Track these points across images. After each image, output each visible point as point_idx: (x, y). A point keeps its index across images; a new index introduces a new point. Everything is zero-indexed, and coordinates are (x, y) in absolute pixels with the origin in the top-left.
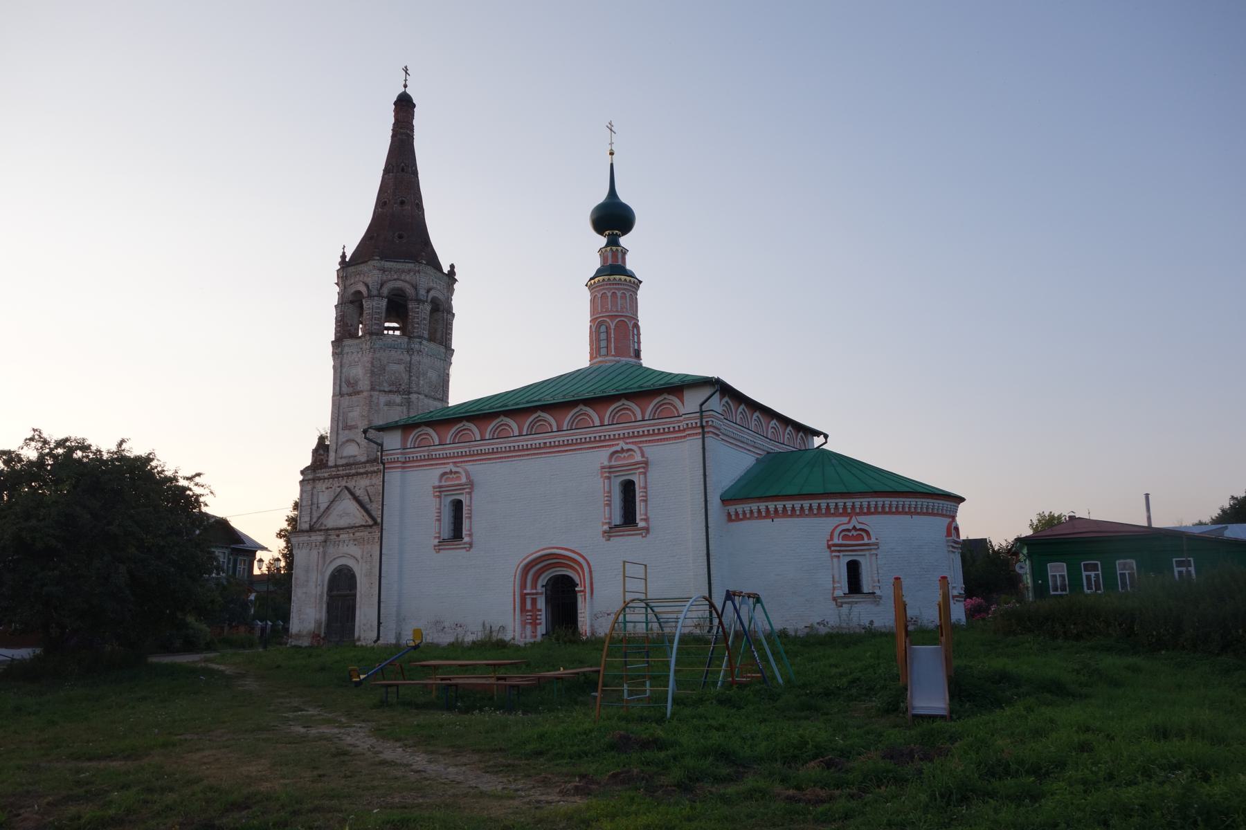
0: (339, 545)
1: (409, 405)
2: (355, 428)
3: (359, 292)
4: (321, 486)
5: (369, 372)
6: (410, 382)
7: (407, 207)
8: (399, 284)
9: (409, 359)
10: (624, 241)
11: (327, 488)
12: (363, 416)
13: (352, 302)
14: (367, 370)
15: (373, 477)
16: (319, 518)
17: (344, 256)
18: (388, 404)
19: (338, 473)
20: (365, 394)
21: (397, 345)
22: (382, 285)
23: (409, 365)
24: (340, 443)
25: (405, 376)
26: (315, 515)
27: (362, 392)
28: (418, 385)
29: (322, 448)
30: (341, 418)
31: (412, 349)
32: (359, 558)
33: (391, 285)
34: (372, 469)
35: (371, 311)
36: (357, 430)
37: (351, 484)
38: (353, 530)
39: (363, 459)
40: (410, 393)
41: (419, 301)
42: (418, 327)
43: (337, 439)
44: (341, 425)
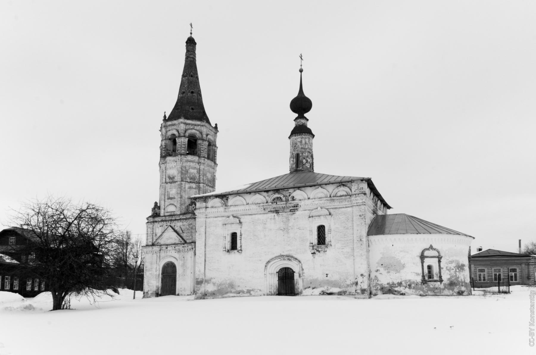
0: (167, 252)
1: (199, 189)
2: (174, 199)
3: (174, 135)
4: (156, 224)
5: (180, 172)
6: (199, 179)
7: (195, 94)
8: (194, 131)
9: (199, 167)
11: (161, 226)
12: (177, 193)
13: (170, 139)
14: (179, 172)
15: (184, 222)
16: (157, 240)
17: (165, 116)
18: (190, 188)
19: (166, 219)
20: (179, 183)
21: (194, 160)
22: (185, 132)
23: (199, 170)
24: (166, 206)
25: (197, 176)
26: (155, 238)
27: (177, 182)
28: (203, 179)
29: (157, 207)
30: (166, 194)
31: (200, 163)
32: (178, 259)
33: (189, 132)
34: (183, 218)
35: (180, 144)
36: (175, 200)
37: (173, 225)
38: (174, 246)
39: (179, 213)
40: (199, 183)
41: (203, 140)
42: (203, 153)
43: (165, 204)
44: (166, 197)
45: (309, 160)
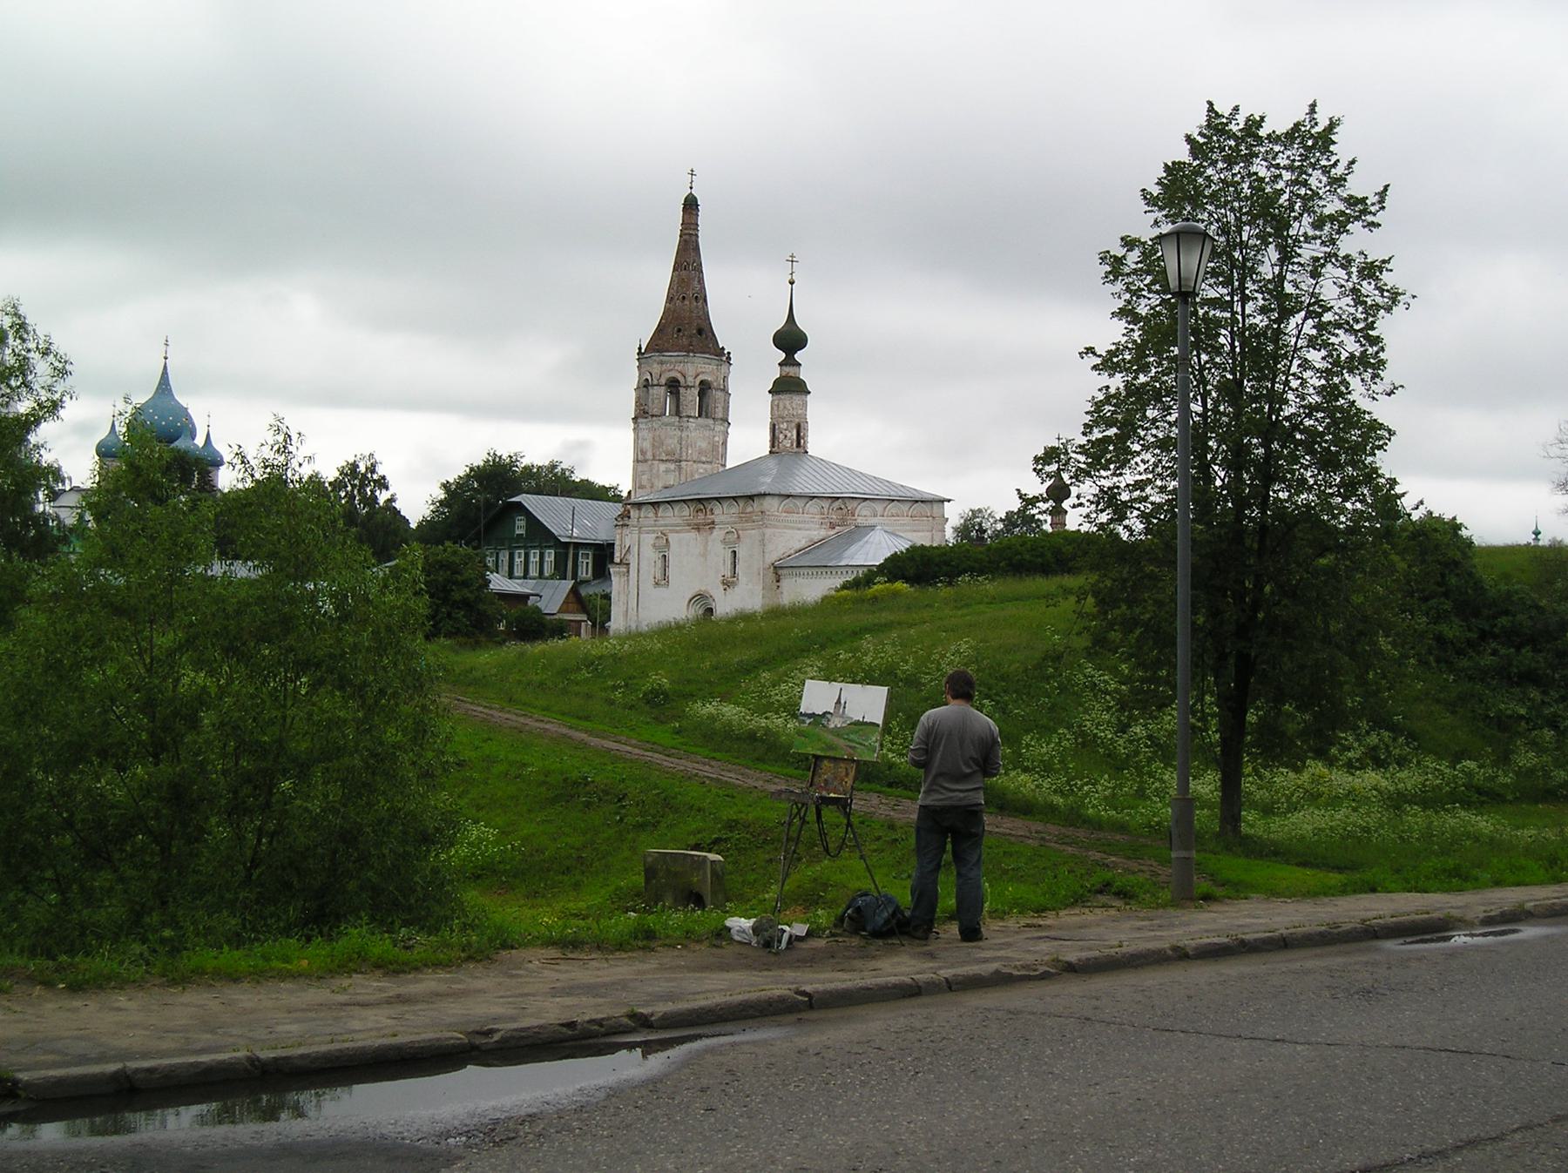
10: (798, 356)
17: (640, 348)
18: (667, 471)
26: (624, 552)
40: (680, 461)
45: (789, 435)
